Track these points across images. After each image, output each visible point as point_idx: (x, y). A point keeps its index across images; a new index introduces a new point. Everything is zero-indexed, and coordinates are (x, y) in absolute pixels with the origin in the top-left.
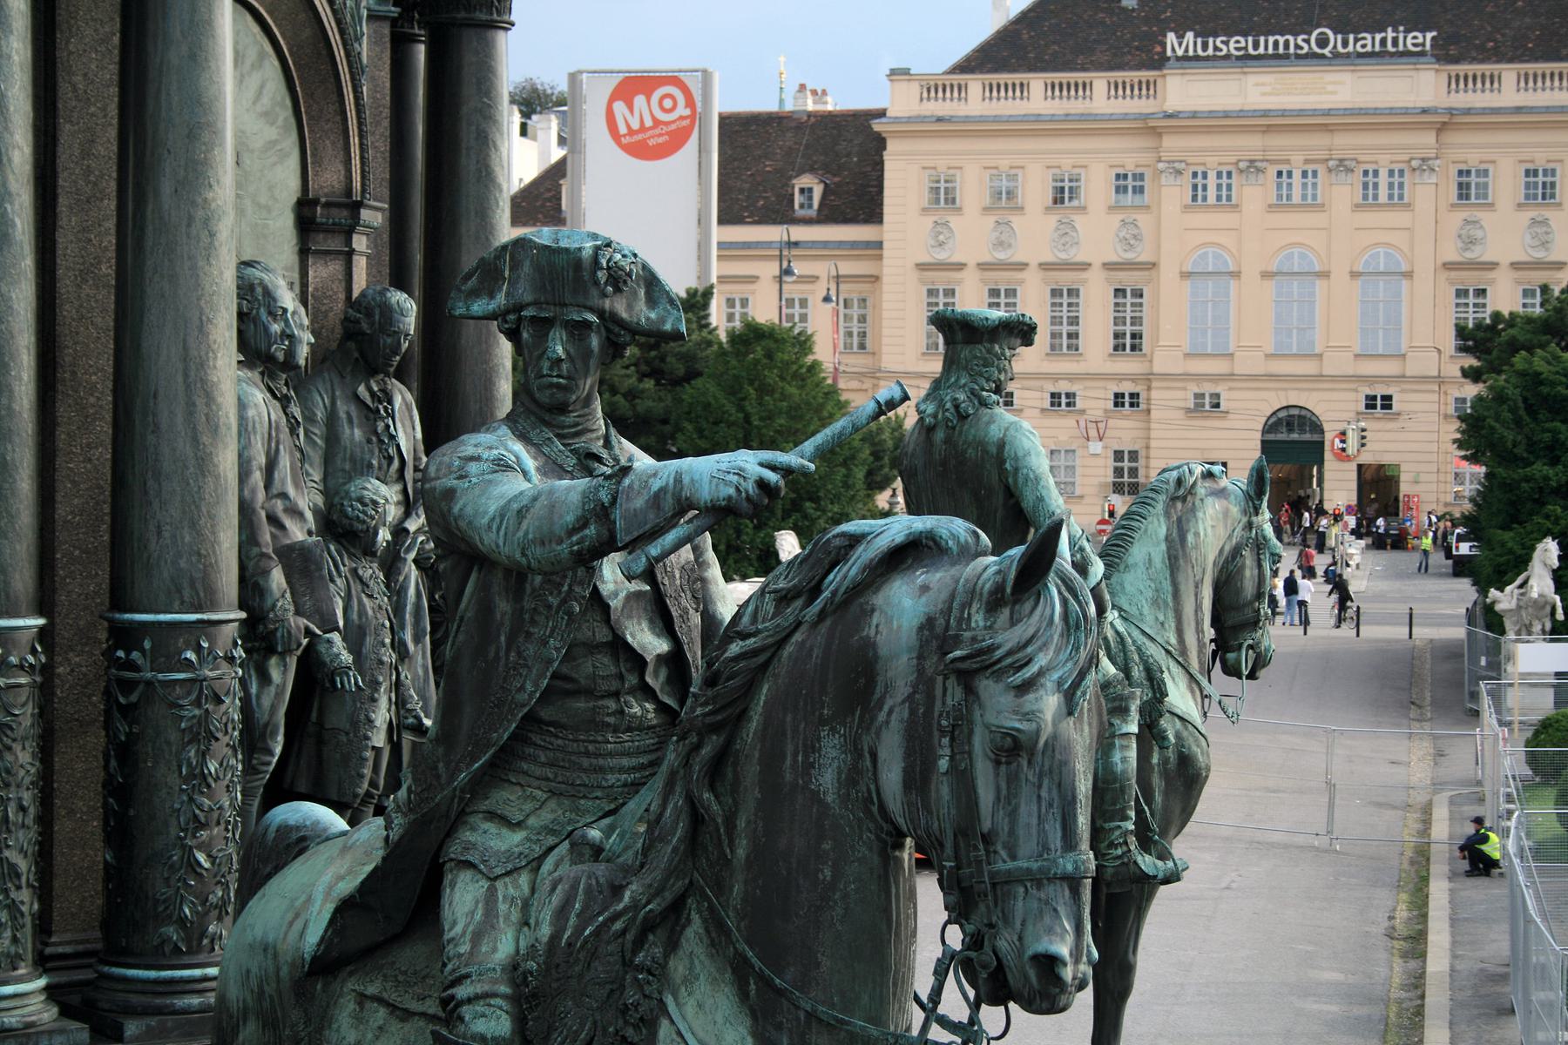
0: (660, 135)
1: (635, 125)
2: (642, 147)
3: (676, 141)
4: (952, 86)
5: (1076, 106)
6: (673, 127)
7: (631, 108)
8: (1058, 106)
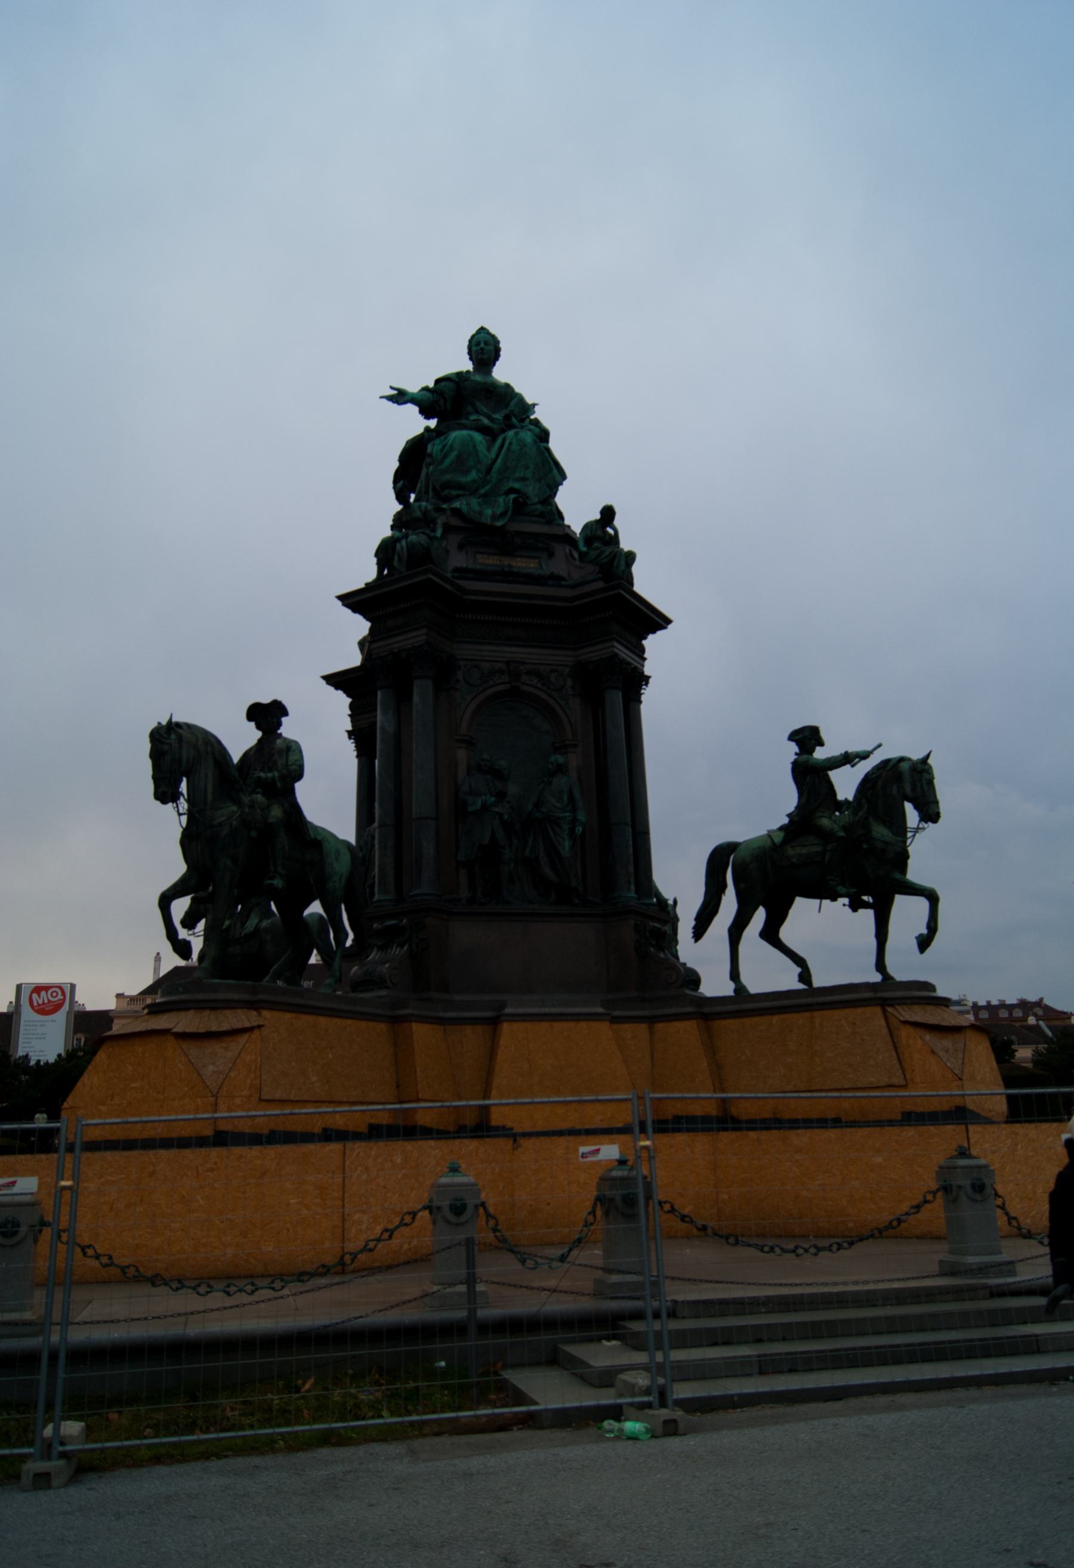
0: (51, 1006)
1: (40, 1002)
3: (57, 1007)
6: (56, 1003)
7: (39, 996)
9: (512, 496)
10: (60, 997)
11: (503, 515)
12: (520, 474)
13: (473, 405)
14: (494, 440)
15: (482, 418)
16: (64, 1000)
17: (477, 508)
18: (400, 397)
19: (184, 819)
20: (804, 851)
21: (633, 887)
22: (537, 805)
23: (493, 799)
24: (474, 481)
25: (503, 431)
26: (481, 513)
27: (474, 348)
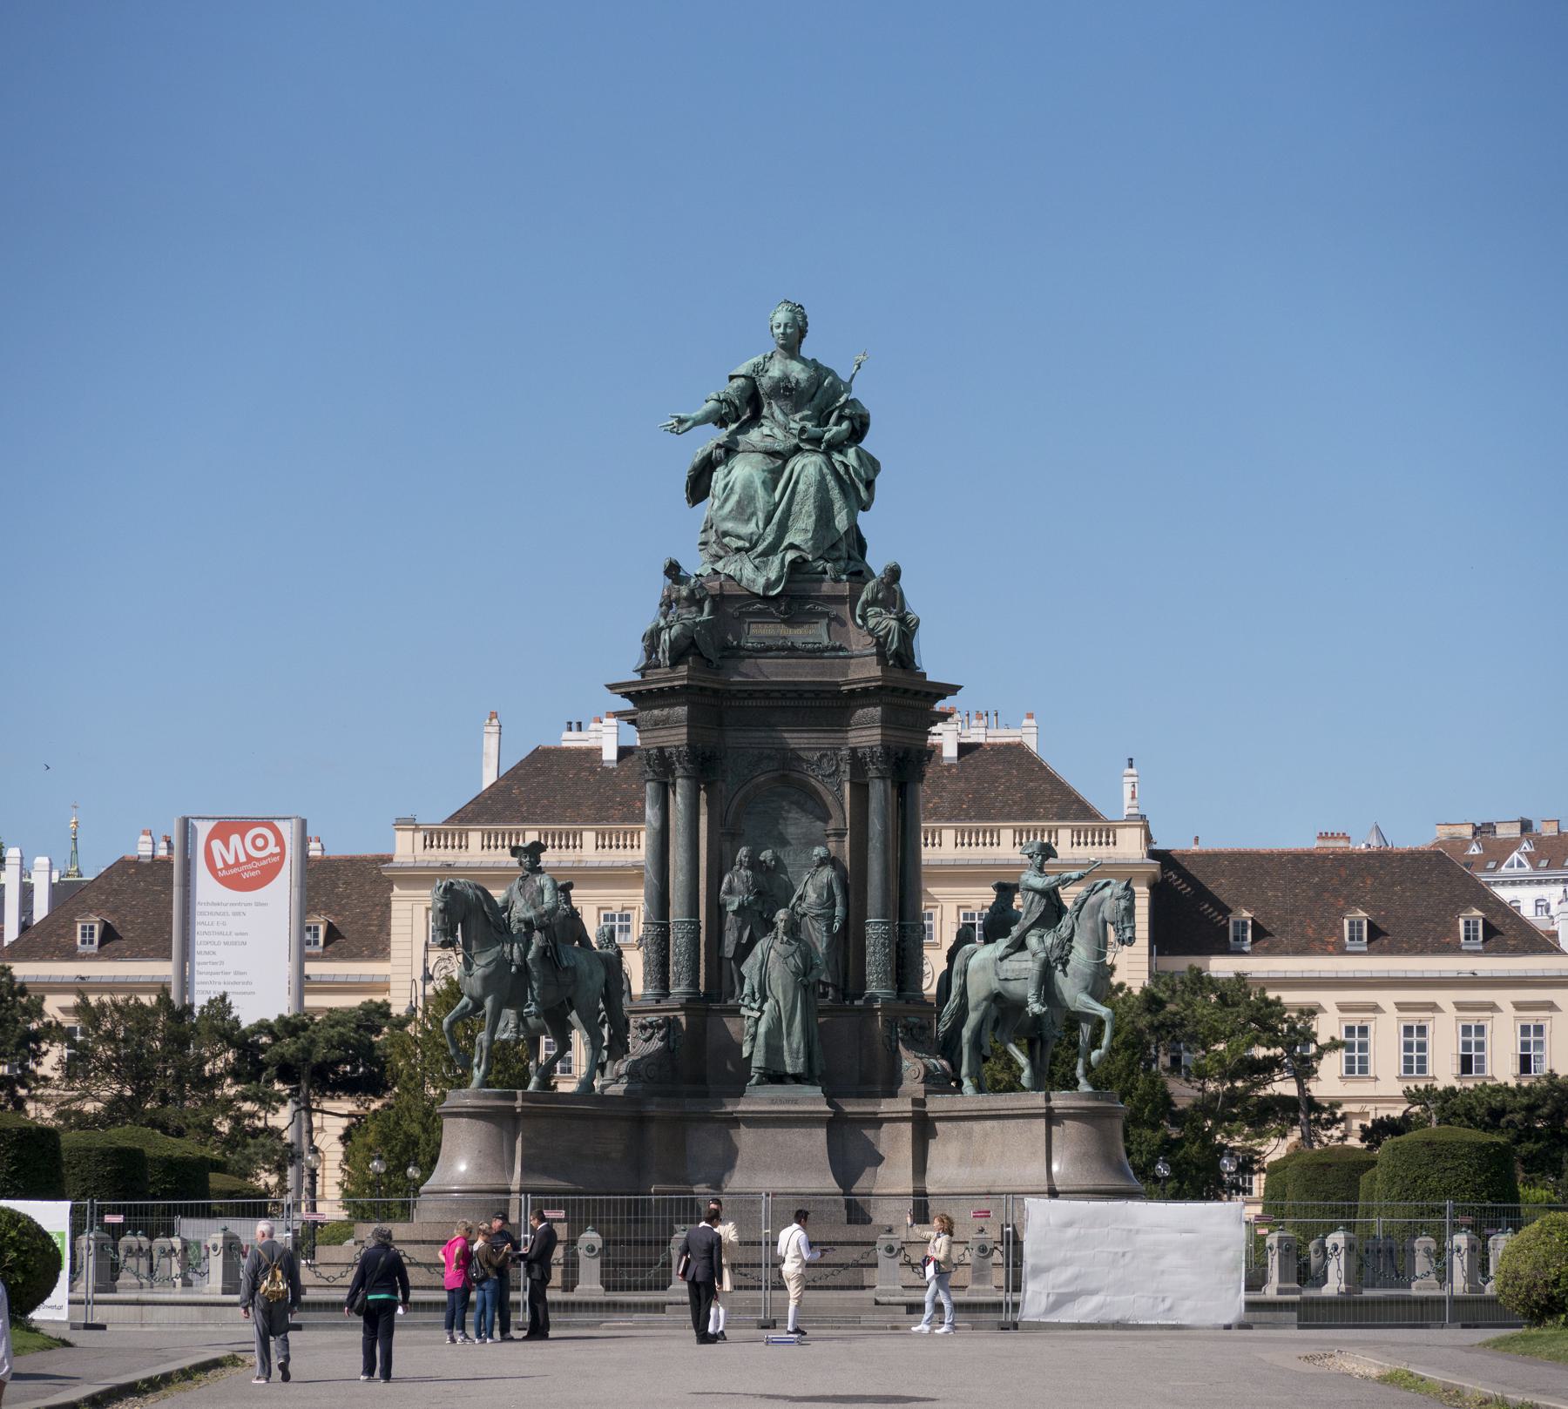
1: (231, 860)
2: (242, 879)
3: (268, 873)
6: (264, 863)
7: (227, 846)
9: (790, 556)
10: (273, 848)
11: (778, 580)
14: (786, 462)
15: (778, 433)
16: (282, 854)
20: (1016, 965)
22: (800, 898)
24: (752, 534)
25: (797, 450)
26: (754, 581)
27: (775, 329)
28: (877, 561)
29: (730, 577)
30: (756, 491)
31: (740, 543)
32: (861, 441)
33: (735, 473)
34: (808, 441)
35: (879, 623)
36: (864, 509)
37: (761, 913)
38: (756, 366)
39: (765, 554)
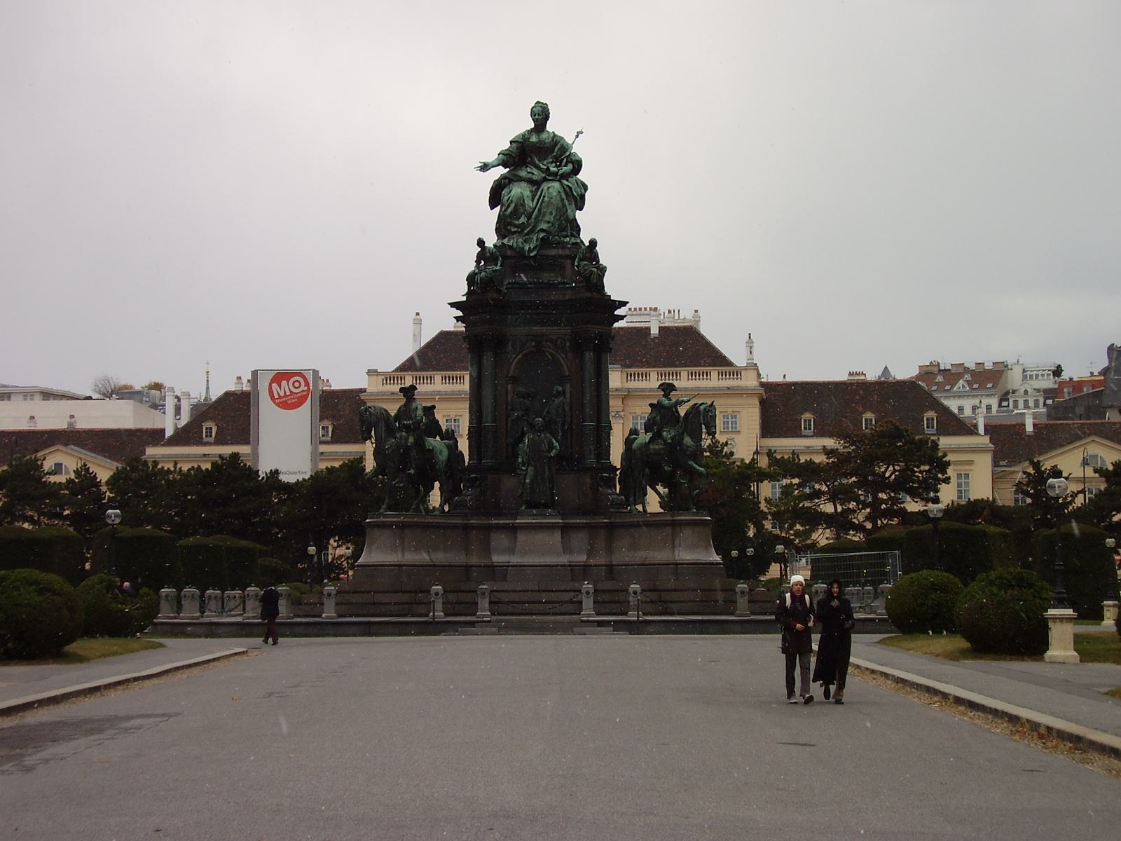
0: (294, 399)
1: (282, 394)
2: (287, 404)
4: (398, 378)
5: (457, 387)
6: (299, 395)
8: (448, 387)
9: (542, 235)
10: (303, 388)
12: (547, 218)
13: (532, 159)
16: (309, 388)
17: (521, 245)
18: (485, 167)
19: (374, 445)
20: (656, 447)
21: (593, 456)
22: (548, 412)
23: (523, 413)
25: (545, 180)
26: (523, 248)
28: (585, 238)
29: (511, 247)
30: (524, 201)
31: (516, 229)
32: (578, 174)
33: (513, 193)
34: (549, 175)
35: (587, 269)
36: (581, 209)
37: (528, 421)
38: (523, 135)
39: (528, 234)
